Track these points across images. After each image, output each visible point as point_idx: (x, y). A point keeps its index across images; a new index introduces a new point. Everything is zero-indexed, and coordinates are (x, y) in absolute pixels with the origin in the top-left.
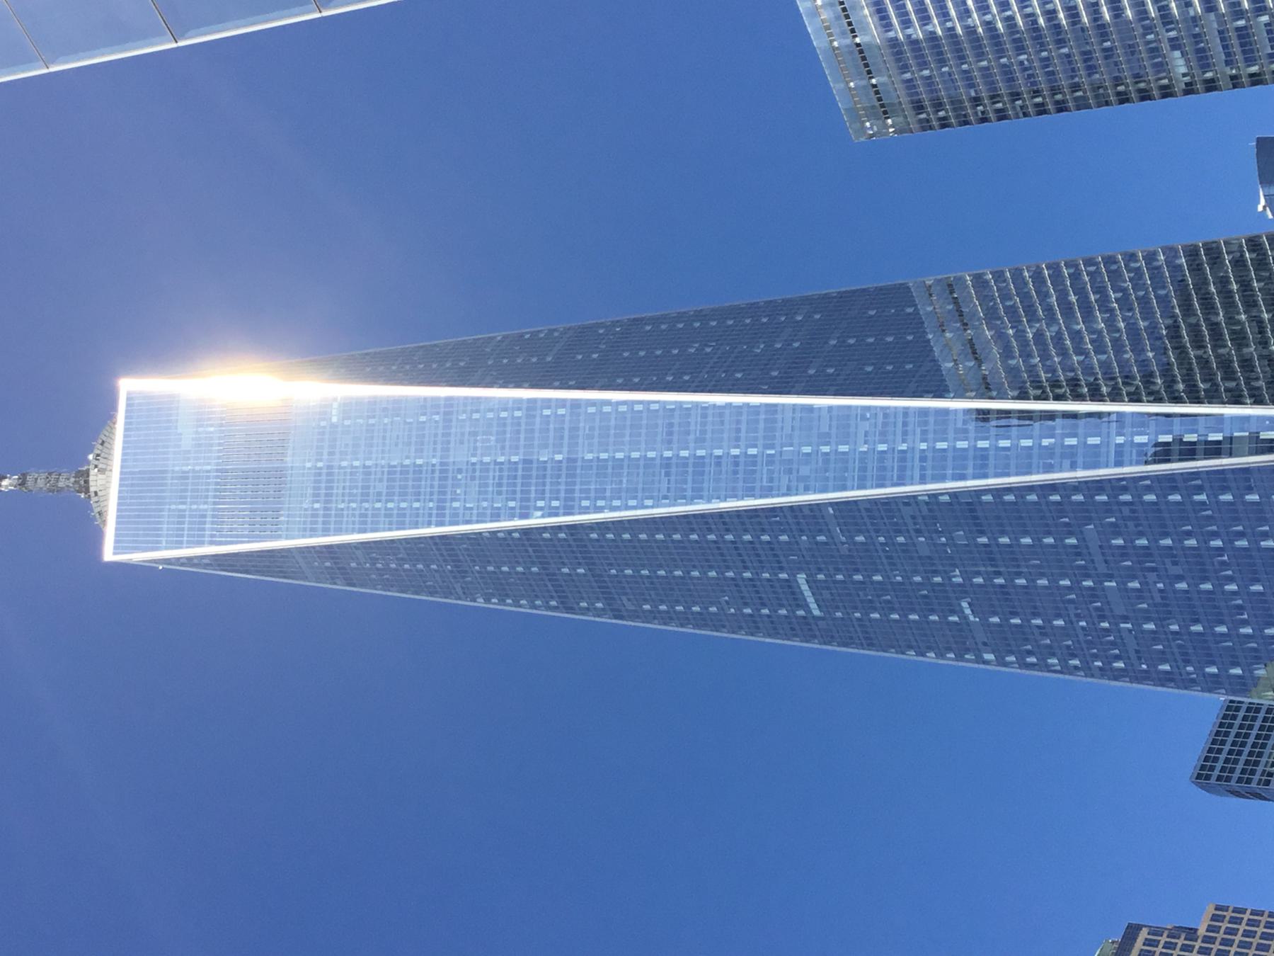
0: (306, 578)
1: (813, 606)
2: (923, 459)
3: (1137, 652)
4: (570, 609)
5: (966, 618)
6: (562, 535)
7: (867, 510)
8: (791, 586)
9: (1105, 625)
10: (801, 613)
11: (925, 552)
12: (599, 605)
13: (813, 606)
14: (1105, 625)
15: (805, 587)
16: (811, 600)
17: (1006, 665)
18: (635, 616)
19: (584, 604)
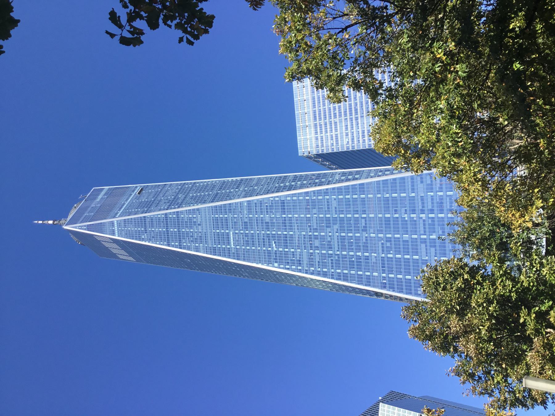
0: (106, 234)
1: (232, 243)
2: (275, 188)
3: (319, 262)
4: (169, 245)
5: (273, 248)
6: (174, 216)
7: (256, 204)
8: (228, 234)
9: (311, 251)
10: (228, 247)
11: (267, 220)
12: (177, 244)
13: (232, 243)
14: (311, 251)
15: (232, 235)
16: (232, 241)
17: (280, 268)
18: (184, 248)
19: (173, 244)
